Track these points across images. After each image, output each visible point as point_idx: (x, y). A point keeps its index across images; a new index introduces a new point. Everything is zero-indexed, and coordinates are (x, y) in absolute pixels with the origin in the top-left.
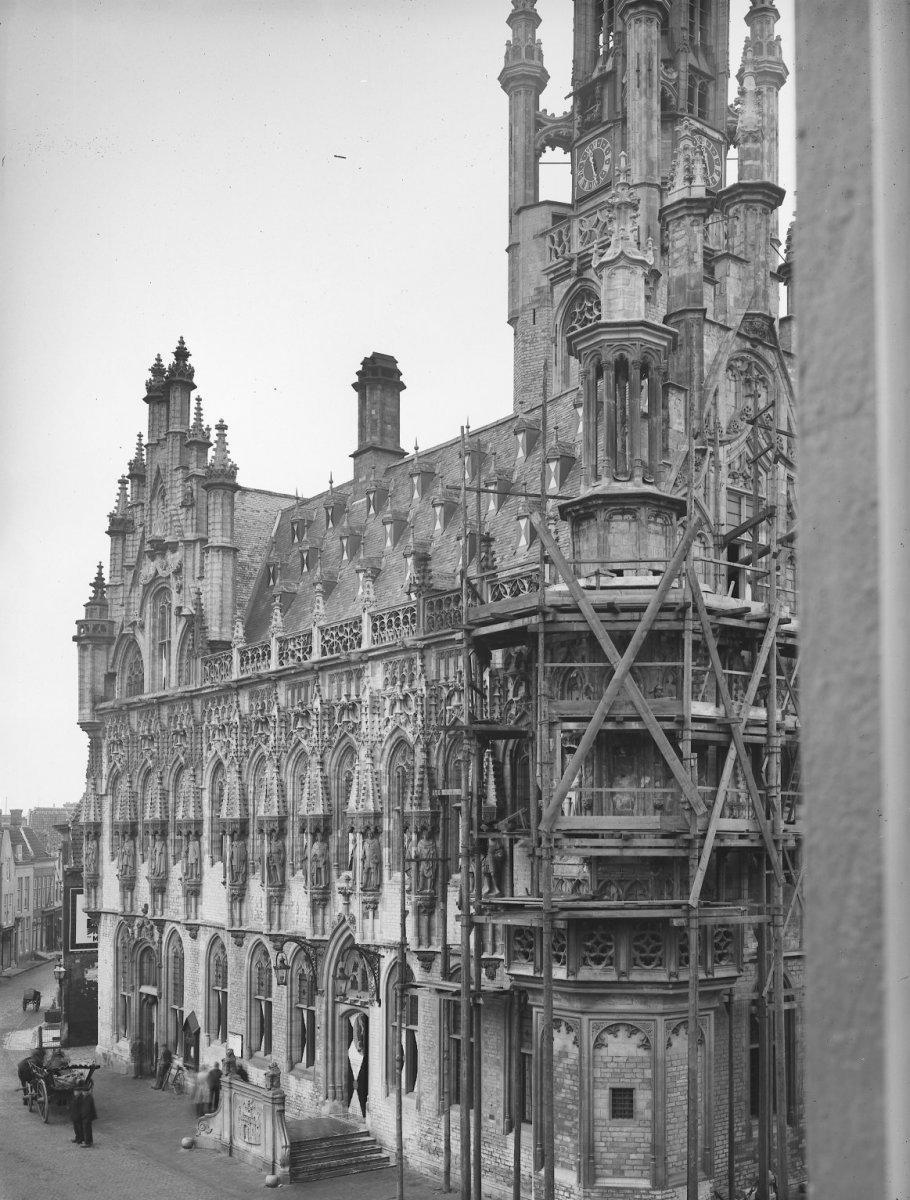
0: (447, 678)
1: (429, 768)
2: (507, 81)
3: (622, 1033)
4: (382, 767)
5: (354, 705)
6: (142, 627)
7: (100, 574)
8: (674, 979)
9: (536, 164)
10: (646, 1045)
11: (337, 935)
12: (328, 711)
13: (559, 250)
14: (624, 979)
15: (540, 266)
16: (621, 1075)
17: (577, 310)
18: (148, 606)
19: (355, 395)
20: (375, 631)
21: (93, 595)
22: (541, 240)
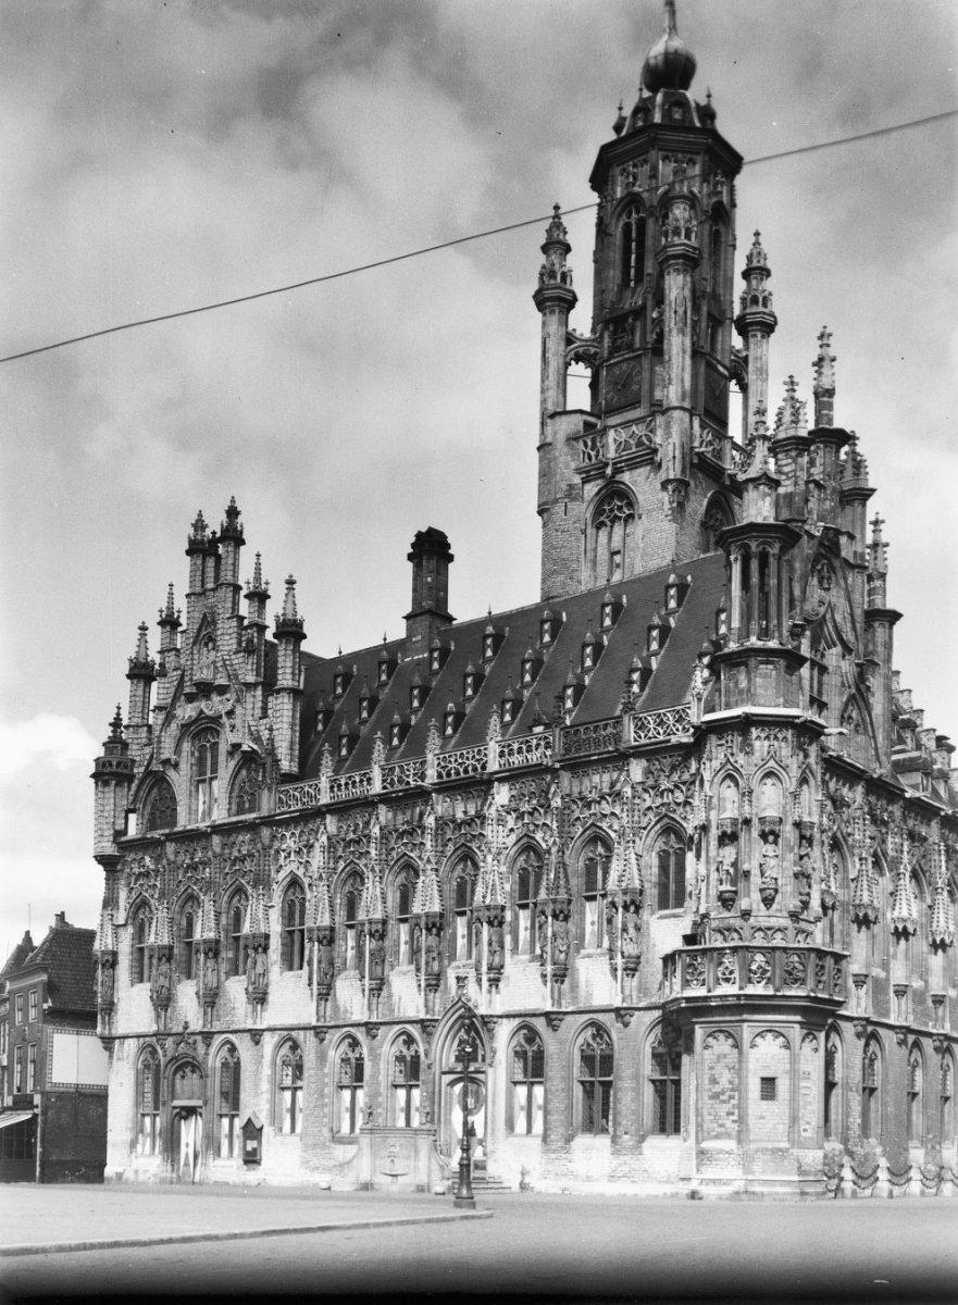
2: (541, 301)
3: (769, 1036)
4: (503, 869)
6: (176, 766)
7: (118, 714)
8: (812, 994)
9: (565, 375)
11: (448, 1016)
12: (442, 823)
13: (593, 453)
14: (778, 994)
15: (573, 465)
18: (186, 746)
19: (410, 565)
20: (501, 756)
21: (111, 735)
22: (574, 443)
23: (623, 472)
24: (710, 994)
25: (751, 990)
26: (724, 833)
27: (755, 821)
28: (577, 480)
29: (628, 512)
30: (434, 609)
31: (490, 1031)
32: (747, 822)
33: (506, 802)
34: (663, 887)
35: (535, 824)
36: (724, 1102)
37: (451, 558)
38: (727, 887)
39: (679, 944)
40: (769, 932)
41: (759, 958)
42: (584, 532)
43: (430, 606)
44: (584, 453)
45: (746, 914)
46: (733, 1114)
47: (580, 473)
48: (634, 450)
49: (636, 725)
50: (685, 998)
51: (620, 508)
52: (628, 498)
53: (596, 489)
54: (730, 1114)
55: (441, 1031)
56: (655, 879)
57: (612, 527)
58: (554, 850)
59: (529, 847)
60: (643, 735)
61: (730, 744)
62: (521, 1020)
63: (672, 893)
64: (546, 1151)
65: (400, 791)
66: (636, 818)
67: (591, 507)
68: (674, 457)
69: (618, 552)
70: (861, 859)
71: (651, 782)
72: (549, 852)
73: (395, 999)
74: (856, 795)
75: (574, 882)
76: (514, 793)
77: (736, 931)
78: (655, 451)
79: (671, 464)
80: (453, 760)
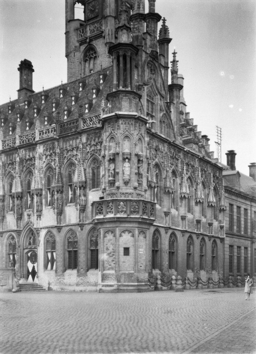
1: (61, 173)
3: (127, 233)
4: (42, 176)
5: (31, 158)
8: (141, 217)
9: (74, 7)
10: (133, 236)
11: (25, 229)
12: (21, 161)
13: (82, 35)
14: (129, 217)
16: (126, 244)
17: (88, 54)
19: (18, 72)
20: (40, 135)
23: (93, 41)
24: (105, 217)
25: (118, 215)
26: (110, 159)
27: (121, 154)
28: (77, 44)
29: (95, 55)
30: (26, 87)
31: (38, 234)
32: (118, 154)
34: (93, 180)
35: (52, 159)
37: (33, 71)
38: (111, 179)
39: (98, 199)
40: (127, 195)
41: (122, 203)
42: (81, 63)
43: (26, 87)
44: (80, 34)
45: (118, 188)
46: (114, 261)
47: (79, 42)
48: (96, 32)
49: (83, 122)
50: (96, 219)
51: (92, 54)
52: (95, 50)
53: (84, 48)
54: (113, 261)
55: (23, 234)
56: (91, 178)
57: (90, 61)
58: (57, 168)
59: (49, 168)
60: (85, 125)
61: (112, 126)
63: (95, 183)
64: (56, 276)
65: (8, 149)
66: (84, 156)
67: (83, 54)
68: (109, 34)
69: (92, 70)
70: (167, 171)
71: (89, 142)
72: (55, 169)
73: (8, 223)
74: (165, 148)
75: (64, 180)
76: (44, 148)
77: (115, 194)
78: (103, 32)
79: (108, 37)
80: (24, 137)
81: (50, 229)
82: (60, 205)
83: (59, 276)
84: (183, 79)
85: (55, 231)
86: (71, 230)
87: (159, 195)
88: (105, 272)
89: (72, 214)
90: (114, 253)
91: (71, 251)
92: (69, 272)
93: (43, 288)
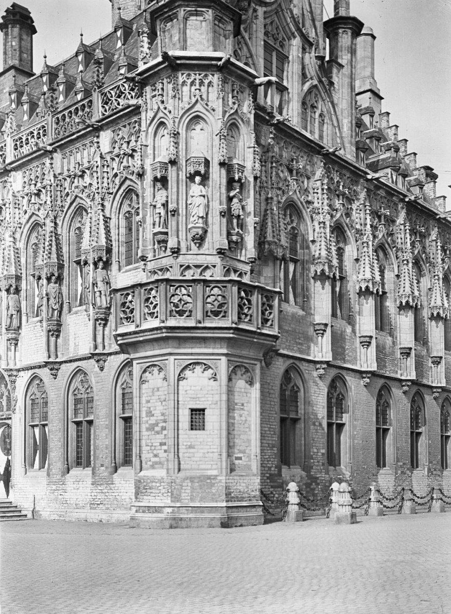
0: (68, 170)
1: (56, 234)
20: (16, 149)
30: (17, 66)
33: (20, 188)
36: (158, 433)
46: (165, 444)
54: (161, 444)
62: (31, 372)
66: (105, 184)
81: (36, 370)
82: (53, 310)
83: (55, 483)
84: (374, 37)
85: (45, 373)
86: (79, 371)
87: (300, 283)
88: (142, 473)
89: (79, 332)
90: (164, 424)
91: (81, 422)
92: (75, 472)
93: (23, 513)
